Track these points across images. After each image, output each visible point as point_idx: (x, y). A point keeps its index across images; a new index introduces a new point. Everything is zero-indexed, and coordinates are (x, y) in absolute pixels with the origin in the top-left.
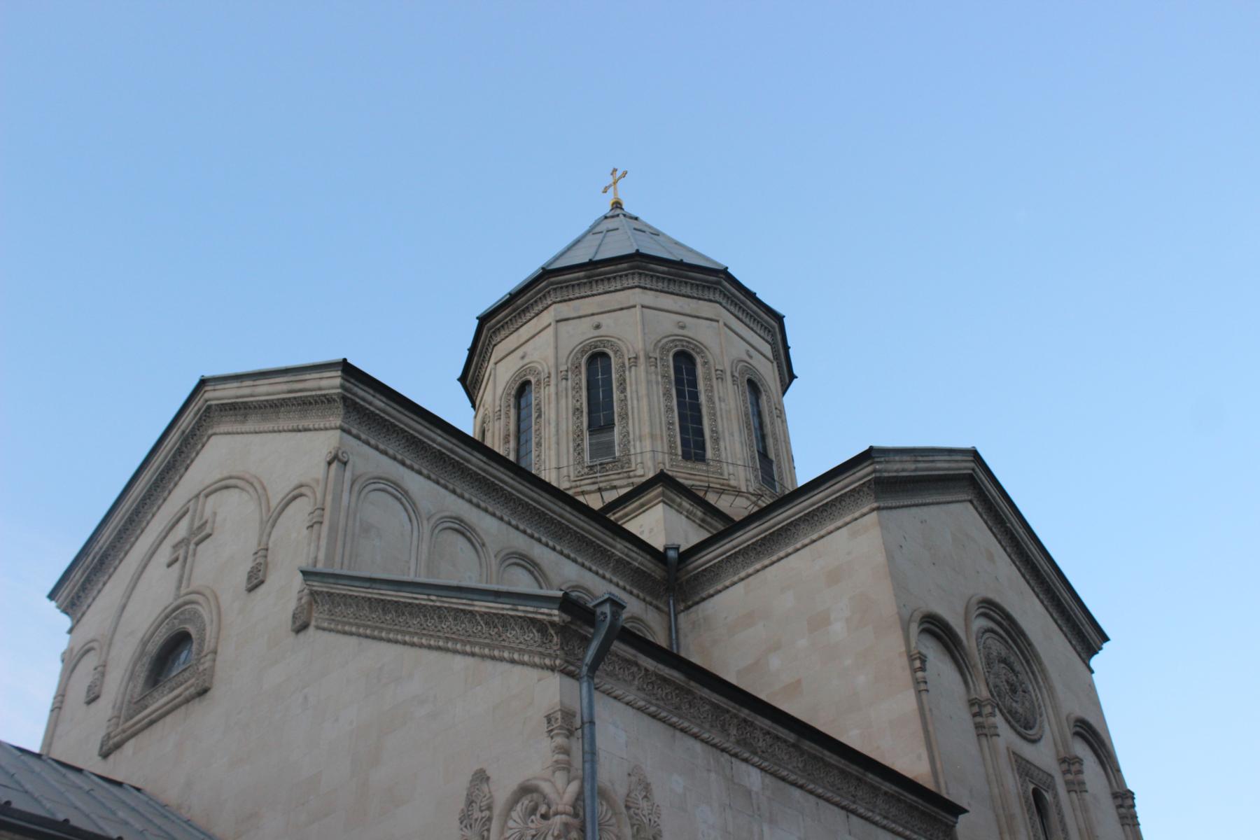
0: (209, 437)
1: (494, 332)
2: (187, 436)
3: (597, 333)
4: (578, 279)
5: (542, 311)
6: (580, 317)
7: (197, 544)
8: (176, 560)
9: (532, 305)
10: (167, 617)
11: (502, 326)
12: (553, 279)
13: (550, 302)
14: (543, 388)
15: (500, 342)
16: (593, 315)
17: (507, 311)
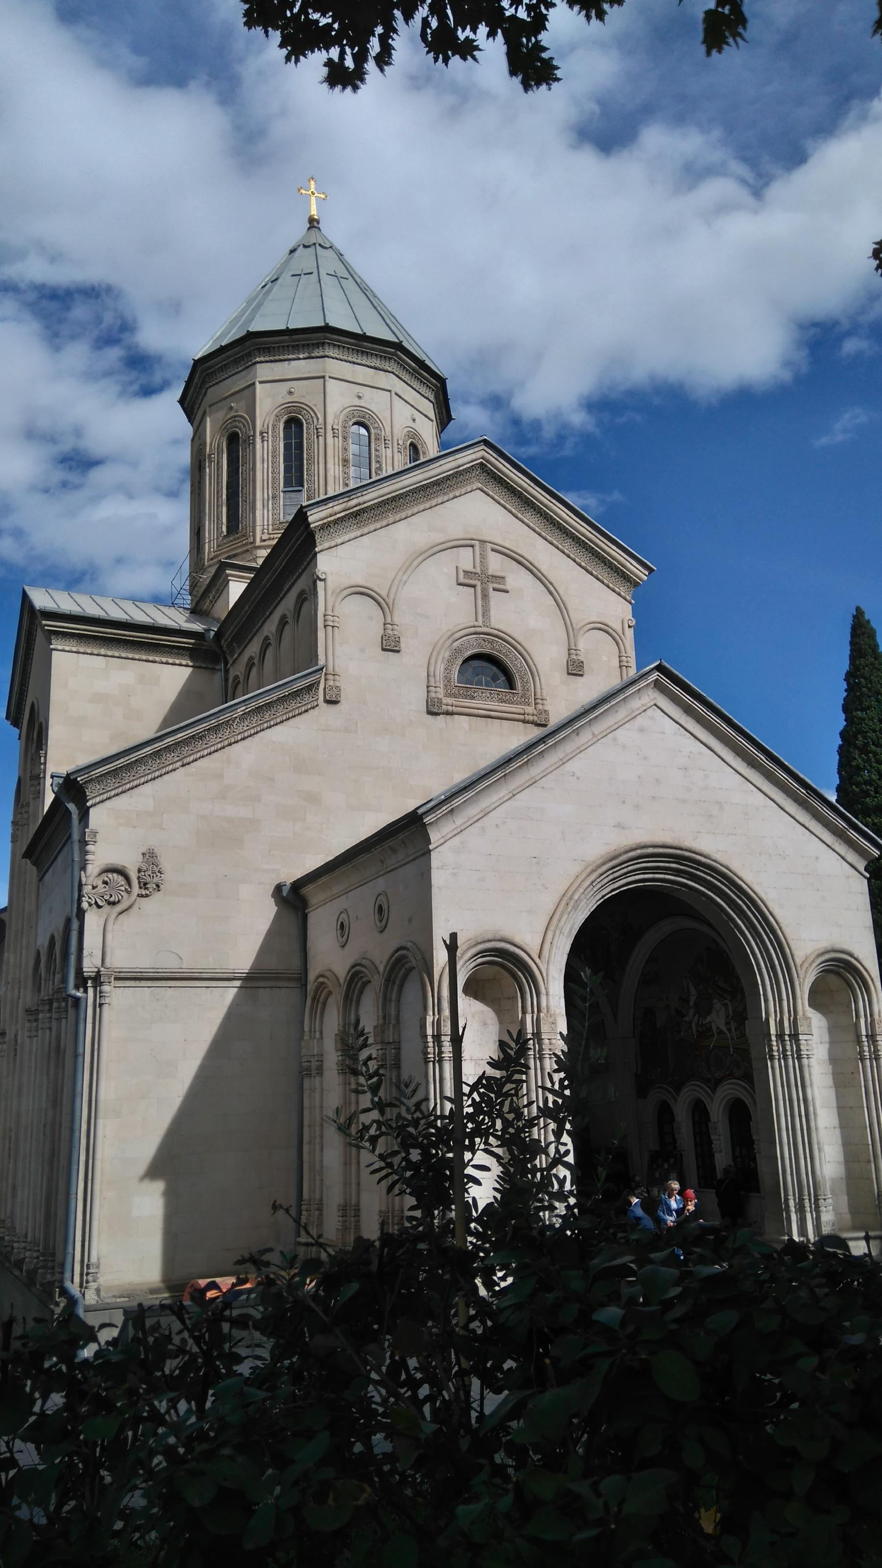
0: (477, 489)
1: (329, 344)
2: (459, 472)
3: (411, 424)
4: (409, 366)
5: (381, 370)
6: (406, 401)
7: (494, 589)
8: (474, 586)
9: (372, 354)
10: (475, 633)
11: (339, 346)
12: (399, 353)
13: (389, 369)
14: (383, 445)
15: (333, 358)
16: (412, 406)
17: (348, 340)
